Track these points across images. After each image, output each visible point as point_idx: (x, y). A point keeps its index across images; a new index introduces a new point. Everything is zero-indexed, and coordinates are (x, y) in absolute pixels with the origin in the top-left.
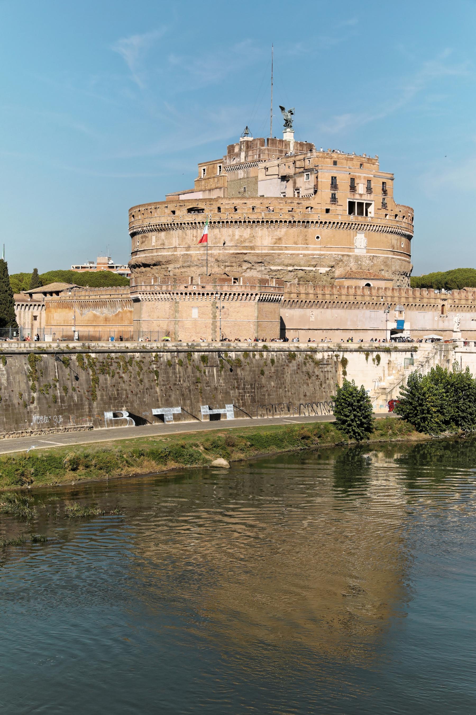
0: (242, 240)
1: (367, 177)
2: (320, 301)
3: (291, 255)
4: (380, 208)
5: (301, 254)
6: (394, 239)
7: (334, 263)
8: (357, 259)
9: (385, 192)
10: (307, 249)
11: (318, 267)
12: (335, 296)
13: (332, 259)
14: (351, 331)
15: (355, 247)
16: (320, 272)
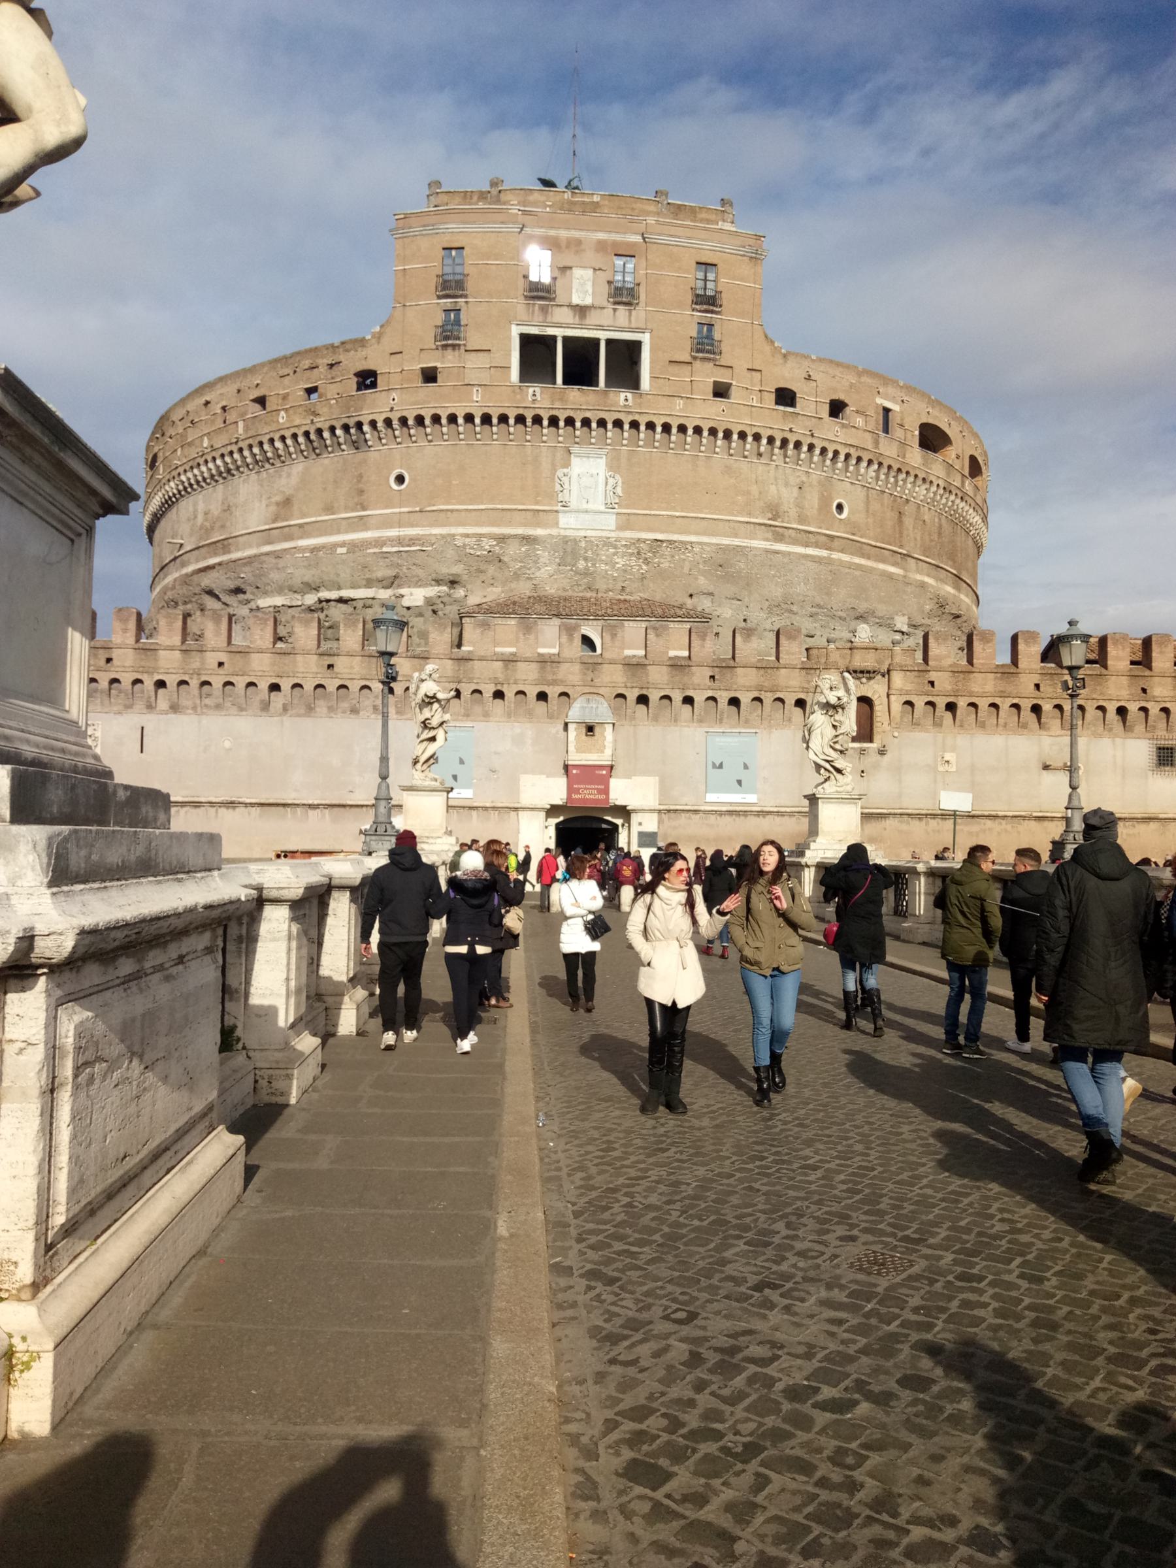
0: (207, 524)
1: (615, 244)
2: (126, 679)
3: (314, 550)
4: (688, 358)
5: (343, 544)
6: (781, 481)
7: (457, 569)
8: (569, 549)
9: (707, 301)
10: (361, 523)
11: (399, 586)
12: (212, 659)
13: (450, 553)
14: (312, 813)
15: (559, 508)
16: (406, 602)
